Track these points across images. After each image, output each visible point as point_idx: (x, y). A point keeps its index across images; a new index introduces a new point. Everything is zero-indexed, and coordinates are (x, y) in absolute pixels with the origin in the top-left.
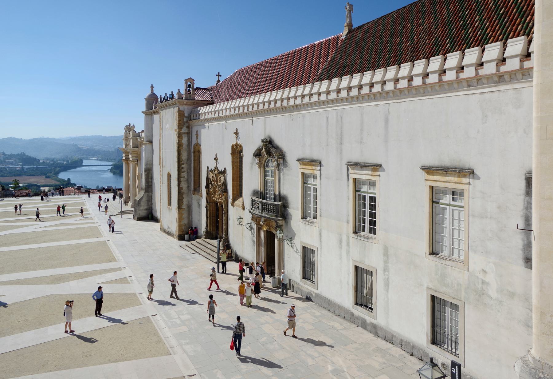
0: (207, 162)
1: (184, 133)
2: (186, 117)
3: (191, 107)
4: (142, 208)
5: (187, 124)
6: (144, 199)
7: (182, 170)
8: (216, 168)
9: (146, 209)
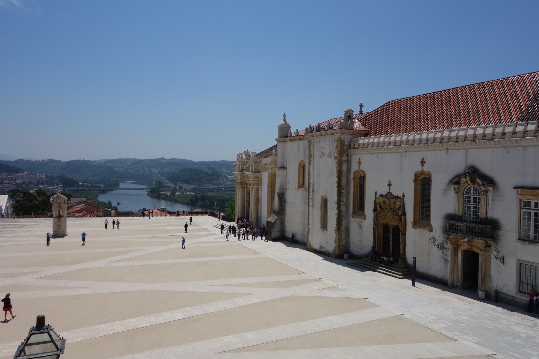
0: (374, 188)
1: (344, 160)
2: (346, 146)
3: (350, 137)
4: (276, 230)
5: (345, 151)
6: (278, 222)
7: (342, 195)
8: (389, 193)
9: (280, 231)
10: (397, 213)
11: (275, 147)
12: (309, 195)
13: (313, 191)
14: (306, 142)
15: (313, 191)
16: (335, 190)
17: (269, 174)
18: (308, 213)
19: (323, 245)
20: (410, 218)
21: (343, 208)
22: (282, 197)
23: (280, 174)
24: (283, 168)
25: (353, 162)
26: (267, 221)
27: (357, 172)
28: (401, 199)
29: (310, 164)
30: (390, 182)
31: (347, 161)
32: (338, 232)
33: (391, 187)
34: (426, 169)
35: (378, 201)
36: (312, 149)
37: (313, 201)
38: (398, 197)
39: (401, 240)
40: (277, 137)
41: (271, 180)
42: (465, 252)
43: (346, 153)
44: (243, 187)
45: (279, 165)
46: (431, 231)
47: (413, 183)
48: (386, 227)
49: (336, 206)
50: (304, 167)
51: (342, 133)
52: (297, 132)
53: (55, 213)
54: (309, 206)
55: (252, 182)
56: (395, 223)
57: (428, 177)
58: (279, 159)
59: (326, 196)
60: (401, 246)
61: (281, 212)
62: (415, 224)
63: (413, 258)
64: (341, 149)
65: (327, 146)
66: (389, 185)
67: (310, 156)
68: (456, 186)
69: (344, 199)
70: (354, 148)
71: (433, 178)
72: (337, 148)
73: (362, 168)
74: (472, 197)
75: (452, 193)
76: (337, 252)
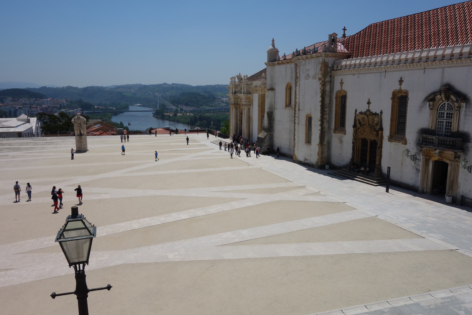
0: (354, 106)
1: (328, 81)
2: (330, 67)
3: (333, 59)
4: (266, 144)
5: (328, 73)
6: (267, 137)
7: (325, 113)
8: (369, 110)
9: (269, 145)
10: (375, 129)
11: (264, 71)
12: (295, 114)
13: (299, 110)
14: (293, 65)
15: (299, 110)
16: (319, 108)
17: (259, 95)
18: (294, 130)
19: (307, 158)
20: (386, 132)
21: (326, 125)
22: (271, 116)
23: (269, 94)
24: (272, 89)
25: (335, 83)
26: (258, 138)
27: (339, 92)
28: (379, 116)
29: (296, 85)
30: (369, 101)
31: (330, 82)
32: (321, 146)
33: (370, 105)
34: (404, 87)
35: (357, 118)
36: (298, 71)
37: (299, 119)
38: (376, 114)
39: (378, 152)
40: (266, 61)
41: (261, 101)
42: (436, 162)
43: (330, 74)
44: (236, 108)
45: (268, 87)
46: (406, 144)
47: (390, 102)
48: (364, 141)
49: (320, 123)
50: (291, 88)
51: (326, 56)
52: (285, 56)
53: (77, 132)
54: (295, 123)
55: (244, 103)
56: (373, 138)
57: (405, 95)
58: (268, 81)
59: (310, 114)
60: (378, 158)
61: (270, 129)
62: (391, 138)
63: (388, 168)
64: (325, 71)
65: (312, 68)
66: (369, 103)
67: (297, 78)
68: (431, 103)
69: (326, 116)
70: (337, 70)
71: (410, 96)
72: (321, 70)
73: (344, 88)
74: (446, 112)
75: (427, 109)
76: (320, 164)
